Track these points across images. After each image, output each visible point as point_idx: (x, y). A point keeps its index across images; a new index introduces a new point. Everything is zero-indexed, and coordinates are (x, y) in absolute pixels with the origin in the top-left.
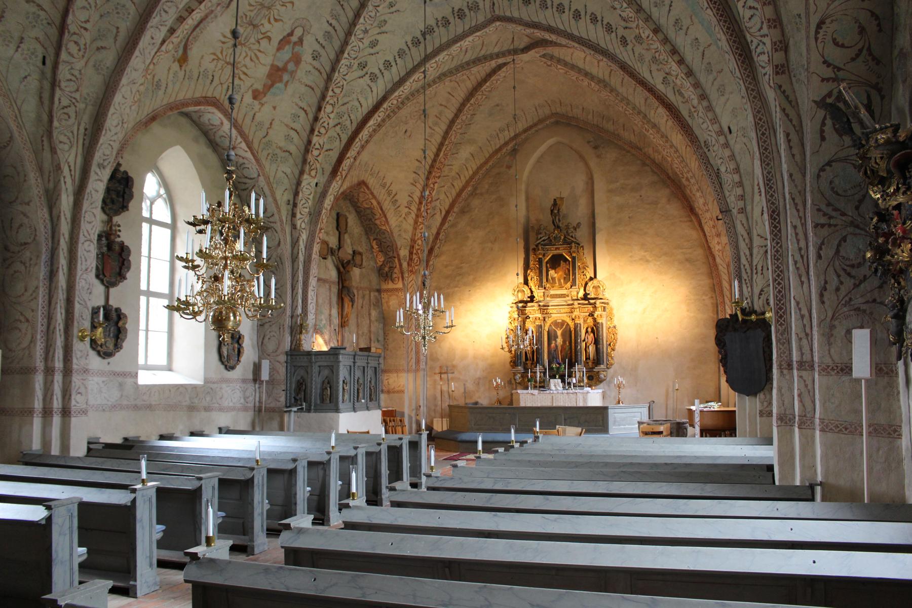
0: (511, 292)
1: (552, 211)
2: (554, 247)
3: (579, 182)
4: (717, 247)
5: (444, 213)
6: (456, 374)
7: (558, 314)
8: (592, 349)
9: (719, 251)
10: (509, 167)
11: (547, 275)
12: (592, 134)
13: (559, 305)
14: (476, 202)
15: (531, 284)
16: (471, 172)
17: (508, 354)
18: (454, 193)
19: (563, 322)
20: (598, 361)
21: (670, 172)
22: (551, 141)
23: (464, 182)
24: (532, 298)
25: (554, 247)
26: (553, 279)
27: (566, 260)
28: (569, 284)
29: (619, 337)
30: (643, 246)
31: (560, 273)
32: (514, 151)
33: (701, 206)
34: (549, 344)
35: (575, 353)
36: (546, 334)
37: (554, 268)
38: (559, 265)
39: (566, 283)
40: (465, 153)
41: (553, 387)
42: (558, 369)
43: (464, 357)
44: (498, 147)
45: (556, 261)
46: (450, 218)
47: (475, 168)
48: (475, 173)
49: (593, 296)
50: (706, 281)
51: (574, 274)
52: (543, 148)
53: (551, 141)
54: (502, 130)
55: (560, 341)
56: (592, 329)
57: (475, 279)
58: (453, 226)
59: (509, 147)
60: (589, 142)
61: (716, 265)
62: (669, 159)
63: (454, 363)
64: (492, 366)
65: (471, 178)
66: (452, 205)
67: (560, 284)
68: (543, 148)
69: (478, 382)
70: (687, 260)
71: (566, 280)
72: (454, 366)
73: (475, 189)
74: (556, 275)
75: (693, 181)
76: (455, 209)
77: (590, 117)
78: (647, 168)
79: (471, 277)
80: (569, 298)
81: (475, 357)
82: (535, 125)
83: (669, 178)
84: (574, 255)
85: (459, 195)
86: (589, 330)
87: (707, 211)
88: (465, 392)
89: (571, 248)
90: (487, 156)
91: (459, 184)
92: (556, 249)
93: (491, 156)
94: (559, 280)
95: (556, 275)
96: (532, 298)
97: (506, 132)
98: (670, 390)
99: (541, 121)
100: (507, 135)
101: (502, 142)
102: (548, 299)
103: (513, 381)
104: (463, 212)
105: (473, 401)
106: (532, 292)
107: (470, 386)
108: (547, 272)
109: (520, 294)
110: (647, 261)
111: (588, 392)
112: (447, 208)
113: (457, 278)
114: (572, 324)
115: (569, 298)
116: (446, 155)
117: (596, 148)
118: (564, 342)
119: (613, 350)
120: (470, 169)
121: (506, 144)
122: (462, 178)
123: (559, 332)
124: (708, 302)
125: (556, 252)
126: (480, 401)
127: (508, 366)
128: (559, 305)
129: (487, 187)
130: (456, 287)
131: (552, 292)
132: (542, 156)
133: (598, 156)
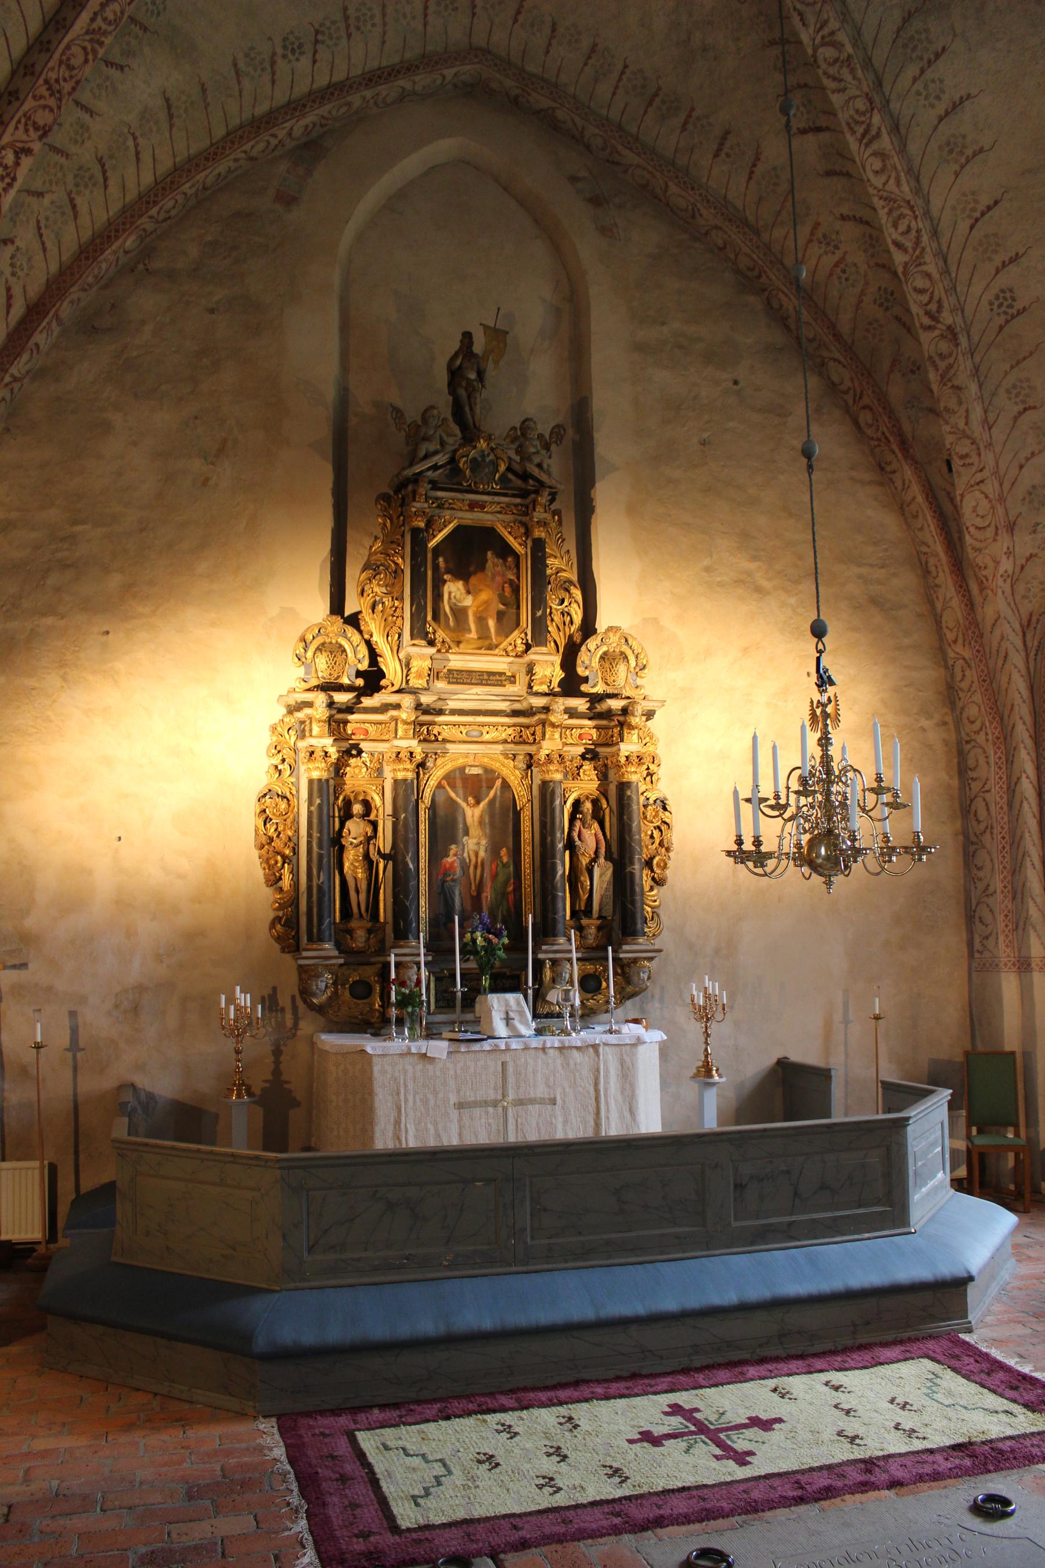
0: (293, 645)
1: (455, 375)
2: (462, 503)
3: (529, 307)
4: (1006, 565)
5: (18, 309)
6: (36, 973)
7: (477, 746)
8: (602, 876)
9: (1005, 576)
10: (287, 200)
11: (438, 597)
12: (588, 149)
13: (468, 710)
14: (146, 302)
15: (372, 625)
16: (148, 179)
17: (267, 895)
18: (71, 238)
19: (490, 776)
20: (624, 916)
21: (844, 323)
22: (444, 148)
23: (115, 208)
24: (372, 679)
25: (462, 503)
26: (460, 613)
27: (505, 551)
28: (517, 639)
29: (676, 837)
30: (745, 538)
31: (484, 596)
32: (311, 150)
33: (976, 428)
34: (437, 853)
35: (547, 896)
36: (423, 816)
37: (462, 574)
38: (482, 567)
39: (505, 631)
40: (149, 80)
41: (500, 1029)
42: (490, 948)
43: (72, 902)
44: (263, 108)
45: (470, 551)
46: (39, 338)
47: (166, 163)
48: (164, 185)
49: (599, 689)
50: (930, 674)
51: (539, 601)
52: (410, 165)
53: (444, 148)
54: (292, 47)
55: (474, 844)
56: (595, 802)
57: (129, 590)
58: (39, 374)
59: (298, 126)
60: (573, 179)
61: (974, 629)
62: (899, 258)
63: (30, 923)
64: (193, 936)
65: (148, 199)
66: (57, 287)
67: (483, 634)
68: (410, 165)
69: (132, 1005)
70: (875, 601)
71: (508, 621)
72: (27, 939)
73: (147, 252)
74: (468, 601)
75: (963, 340)
76: (65, 309)
77: (604, 90)
78: (751, 299)
79: (115, 581)
80: (518, 689)
81: (122, 902)
82: (407, 68)
83: (837, 336)
84: (539, 533)
85: (89, 252)
86: (588, 806)
87: (990, 445)
88: (74, 1046)
89: (526, 511)
90: (220, 132)
91: (97, 209)
92: (473, 506)
93: (235, 137)
94: (481, 620)
95: (468, 601)
96: (372, 679)
97: (305, 61)
98: (838, 1017)
99: (428, 61)
100: (303, 75)
101: (281, 97)
102: (441, 685)
103: (284, 1001)
104: (90, 327)
105: (108, 1083)
106: (374, 655)
107: (98, 1021)
108: (439, 584)
109: (322, 662)
110: (759, 590)
111: (639, 1041)
112: (35, 288)
113: (52, 580)
114: (521, 793)
115: (518, 689)
116: (95, 35)
117: (596, 201)
118: (494, 850)
119: (659, 882)
120: (146, 157)
121: (294, 107)
122: (113, 189)
123: (473, 814)
124: (935, 736)
125: (470, 518)
126: (142, 1081)
127: (263, 935)
128: (468, 710)
129: (194, 251)
130: (51, 610)
131: (456, 661)
132: (402, 194)
133: (605, 231)
